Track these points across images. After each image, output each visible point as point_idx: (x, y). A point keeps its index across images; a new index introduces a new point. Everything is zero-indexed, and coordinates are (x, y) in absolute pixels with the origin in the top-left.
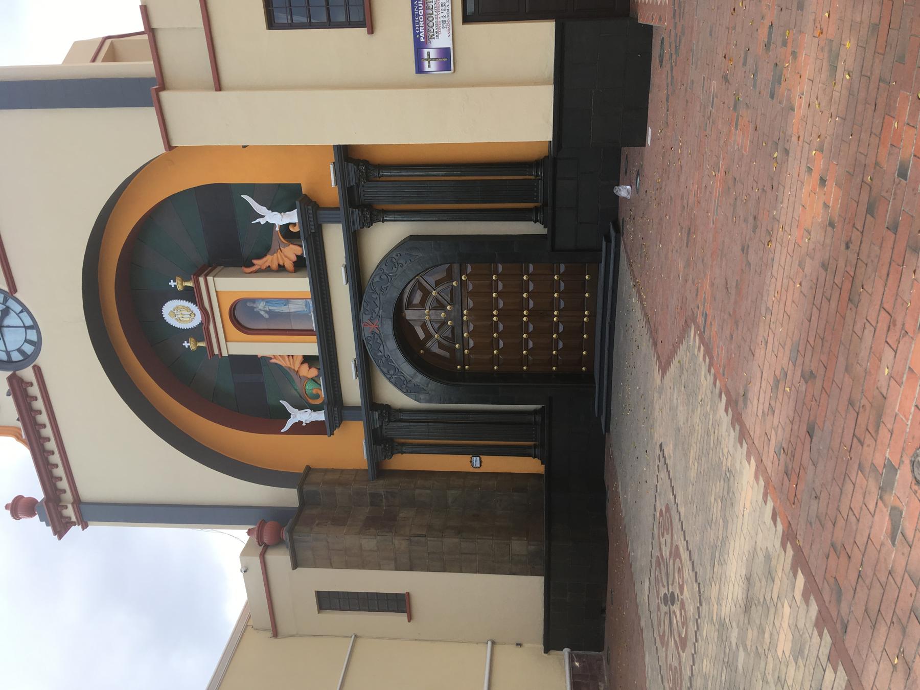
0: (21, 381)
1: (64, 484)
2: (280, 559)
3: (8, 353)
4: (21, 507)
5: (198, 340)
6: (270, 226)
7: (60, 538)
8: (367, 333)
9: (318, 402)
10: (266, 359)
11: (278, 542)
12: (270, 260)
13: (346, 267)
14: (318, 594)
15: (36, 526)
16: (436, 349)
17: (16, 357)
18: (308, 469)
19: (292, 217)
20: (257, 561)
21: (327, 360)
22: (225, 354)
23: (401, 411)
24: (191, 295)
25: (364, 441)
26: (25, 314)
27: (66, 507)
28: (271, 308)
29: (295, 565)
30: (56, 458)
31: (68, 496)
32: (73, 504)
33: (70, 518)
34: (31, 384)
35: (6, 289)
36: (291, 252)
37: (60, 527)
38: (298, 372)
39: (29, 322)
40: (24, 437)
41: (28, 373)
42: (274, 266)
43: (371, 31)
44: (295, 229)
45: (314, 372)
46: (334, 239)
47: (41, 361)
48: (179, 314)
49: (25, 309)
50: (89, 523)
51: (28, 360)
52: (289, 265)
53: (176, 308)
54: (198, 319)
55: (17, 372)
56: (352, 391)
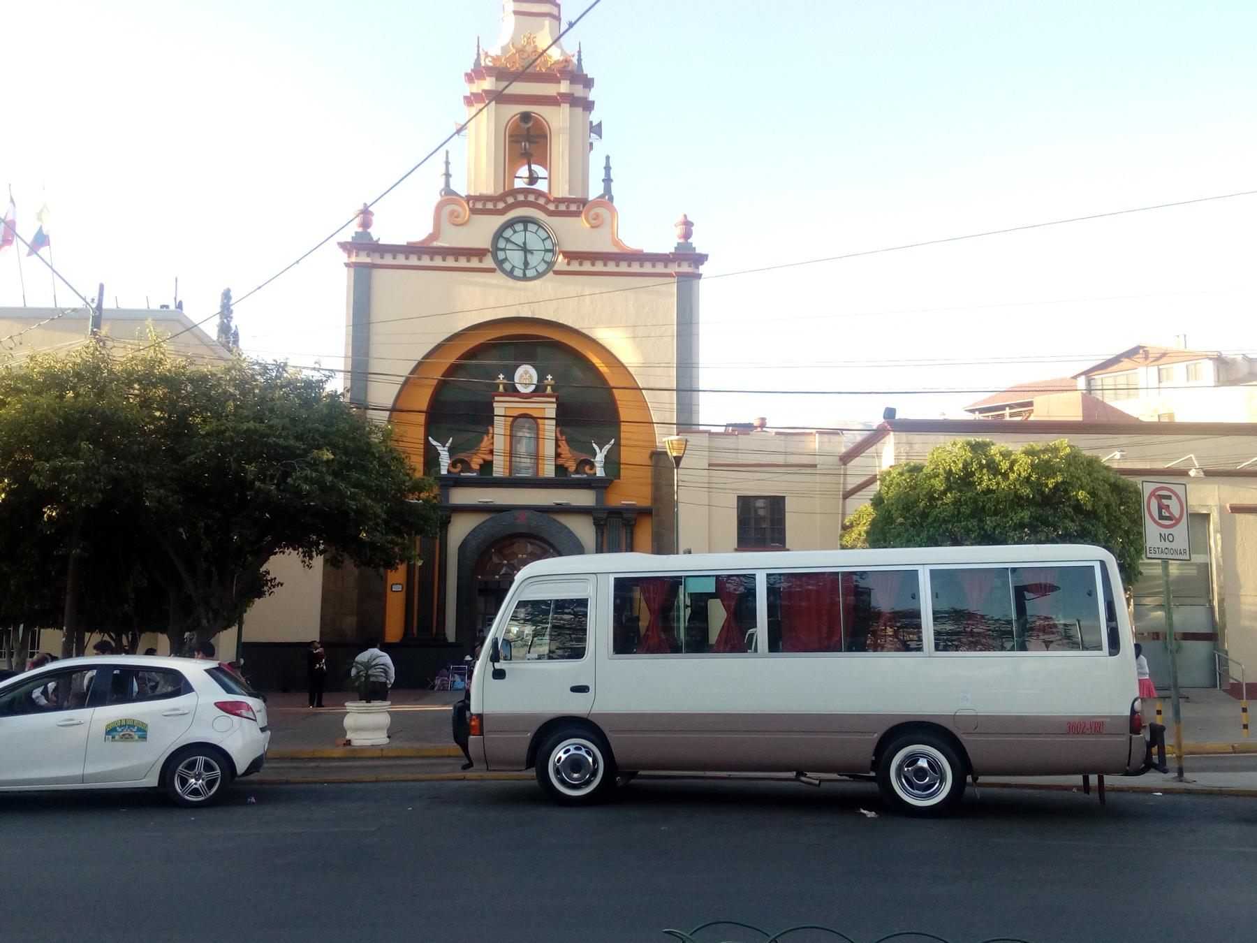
1: (388, 260)
3: (504, 250)
4: (366, 216)
5: (505, 385)
6: (595, 454)
8: (517, 513)
9: (452, 470)
10: (488, 433)
12: (565, 449)
16: (495, 559)
17: (501, 255)
19: (600, 472)
21: (486, 478)
22: (495, 405)
24: (539, 391)
27: (368, 255)
28: (524, 441)
34: (481, 261)
35: (556, 268)
36: (572, 466)
39: (530, 273)
40: (436, 244)
41: (489, 262)
42: (559, 450)
44: (587, 468)
45: (475, 466)
46: (584, 498)
48: (526, 376)
49: (539, 275)
50: (352, 270)
51: (500, 263)
52: (560, 462)
53: (531, 377)
56: (460, 496)
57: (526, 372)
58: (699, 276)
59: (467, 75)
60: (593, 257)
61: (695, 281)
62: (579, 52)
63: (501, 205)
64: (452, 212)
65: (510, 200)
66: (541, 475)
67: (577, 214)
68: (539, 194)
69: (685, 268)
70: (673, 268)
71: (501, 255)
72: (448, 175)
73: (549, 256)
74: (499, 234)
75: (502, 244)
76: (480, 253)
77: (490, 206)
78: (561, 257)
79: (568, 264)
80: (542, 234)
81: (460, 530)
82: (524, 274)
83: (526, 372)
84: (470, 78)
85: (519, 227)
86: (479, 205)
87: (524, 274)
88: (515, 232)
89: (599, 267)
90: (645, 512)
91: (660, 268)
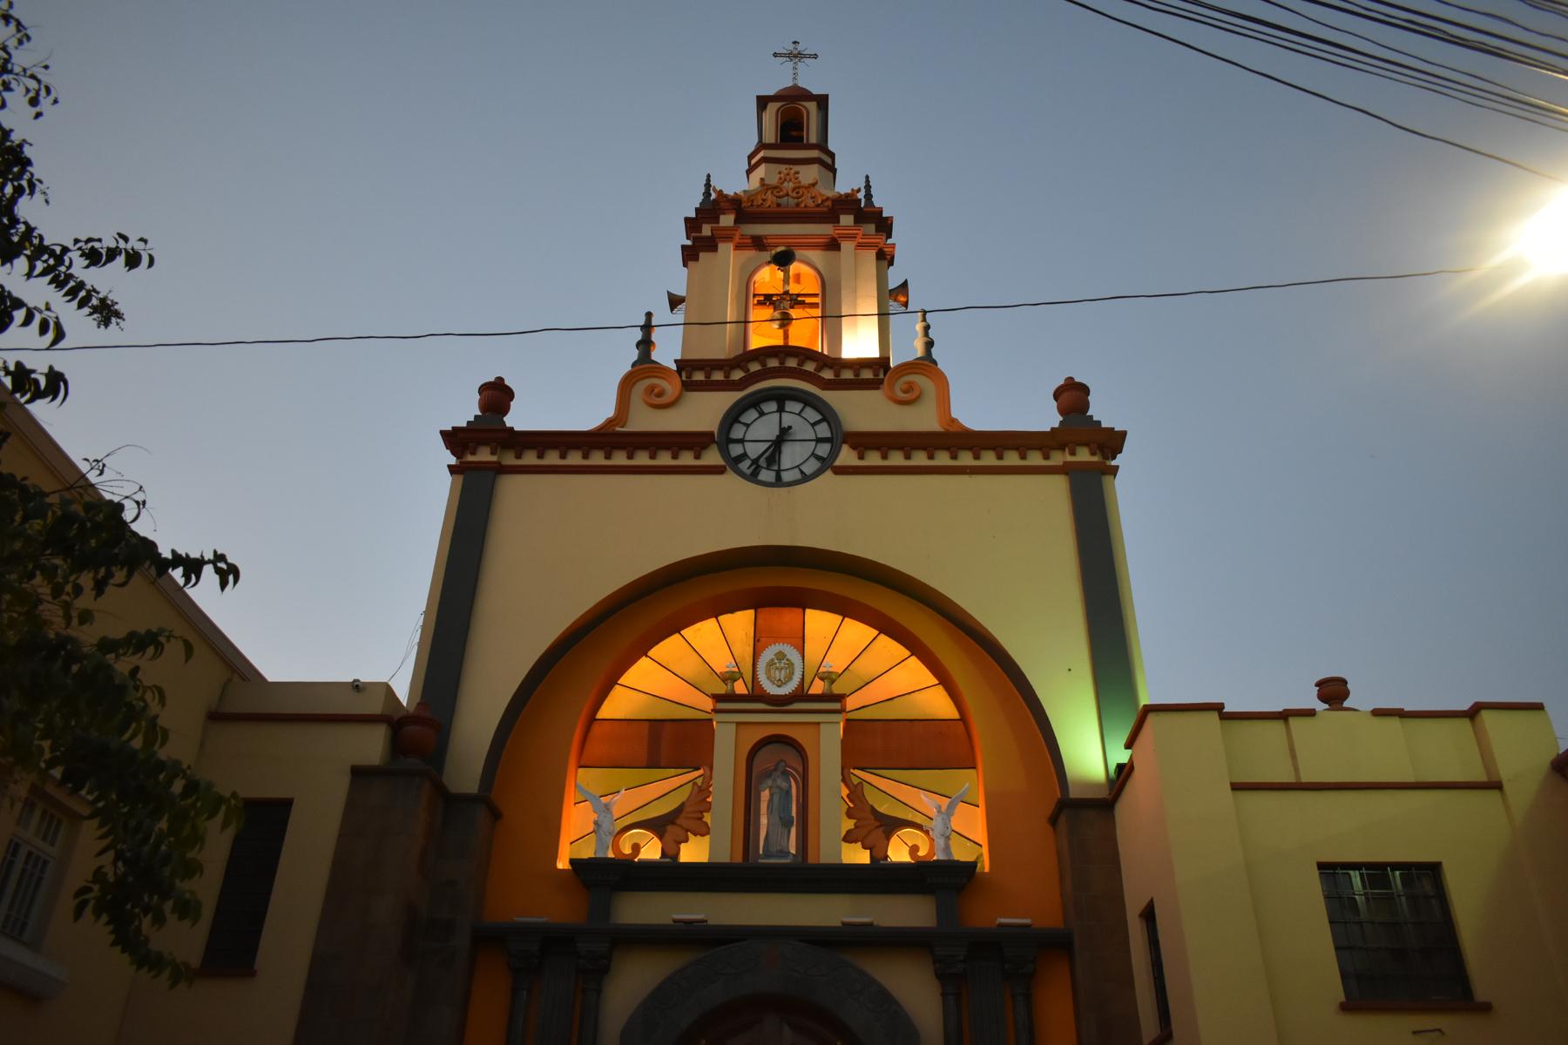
0: (705, 447)
1: (530, 458)
2: (372, 746)
3: (742, 441)
4: (497, 396)
7: (442, 433)
11: (398, 745)
13: (871, 924)
14: (287, 804)
15: (466, 411)
18: (496, 815)
20: (376, 708)
23: (599, 991)
25: (544, 920)
26: (798, 476)
27: (493, 453)
29: (360, 774)
30: (575, 459)
31: (509, 459)
32: (499, 463)
33: (473, 453)
34: (697, 457)
35: (837, 463)
37: (455, 439)
38: (673, 823)
39: (786, 477)
41: (712, 457)
43: (1345, 1008)
46: (911, 912)
47: (730, 478)
49: (806, 478)
50: (460, 478)
53: (791, 665)
54: (772, 690)
55: (715, 447)
56: (641, 910)
57: (781, 656)
58: (1114, 471)
59: (687, 220)
60: (907, 442)
61: (1107, 479)
62: (868, 187)
63: (737, 375)
64: (650, 390)
65: (755, 367)
66: (811, 860)
67: (873, 385)
68: (805, 354)
69: (1083, 455)
70: (1058, 458)
71: (736, 450)
72: (645, 345)
73: (823, 450)
74: (733, 417)
75: (737, 432)
76: (695, 441)
77: (718, 376)
78: (845, 449)
79: (861, 457)
80: (813, 415)
81: (631, 983)
82: (778, 478)
83: (781, 656)
84: (692, 225)
85: (771, 407)
86: (699, 376)
87: (778, 478)
88: (762, 414)
89: (920, 459)
90: (1055, 944)
91: (1035, 459)
